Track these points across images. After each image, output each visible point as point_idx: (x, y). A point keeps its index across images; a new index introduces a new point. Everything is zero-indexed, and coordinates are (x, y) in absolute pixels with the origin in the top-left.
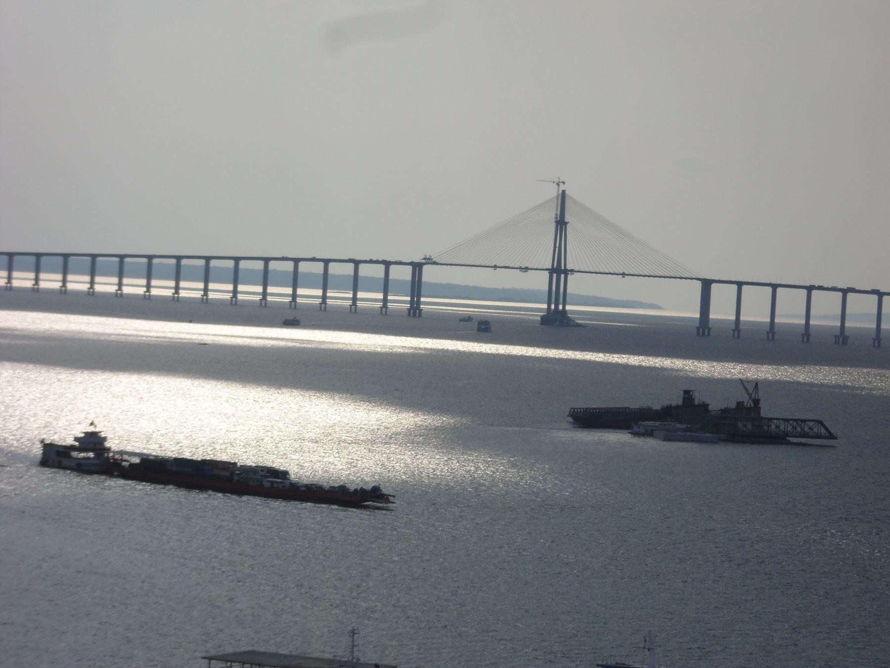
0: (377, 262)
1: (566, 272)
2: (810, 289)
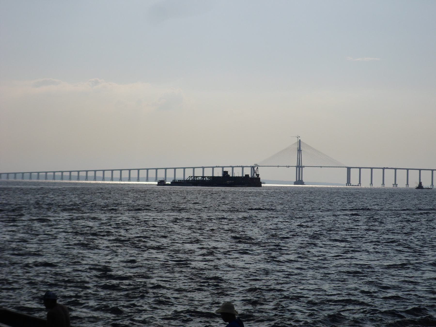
0: (239, 167)
1: (302, 167)
2: (384, 169)
